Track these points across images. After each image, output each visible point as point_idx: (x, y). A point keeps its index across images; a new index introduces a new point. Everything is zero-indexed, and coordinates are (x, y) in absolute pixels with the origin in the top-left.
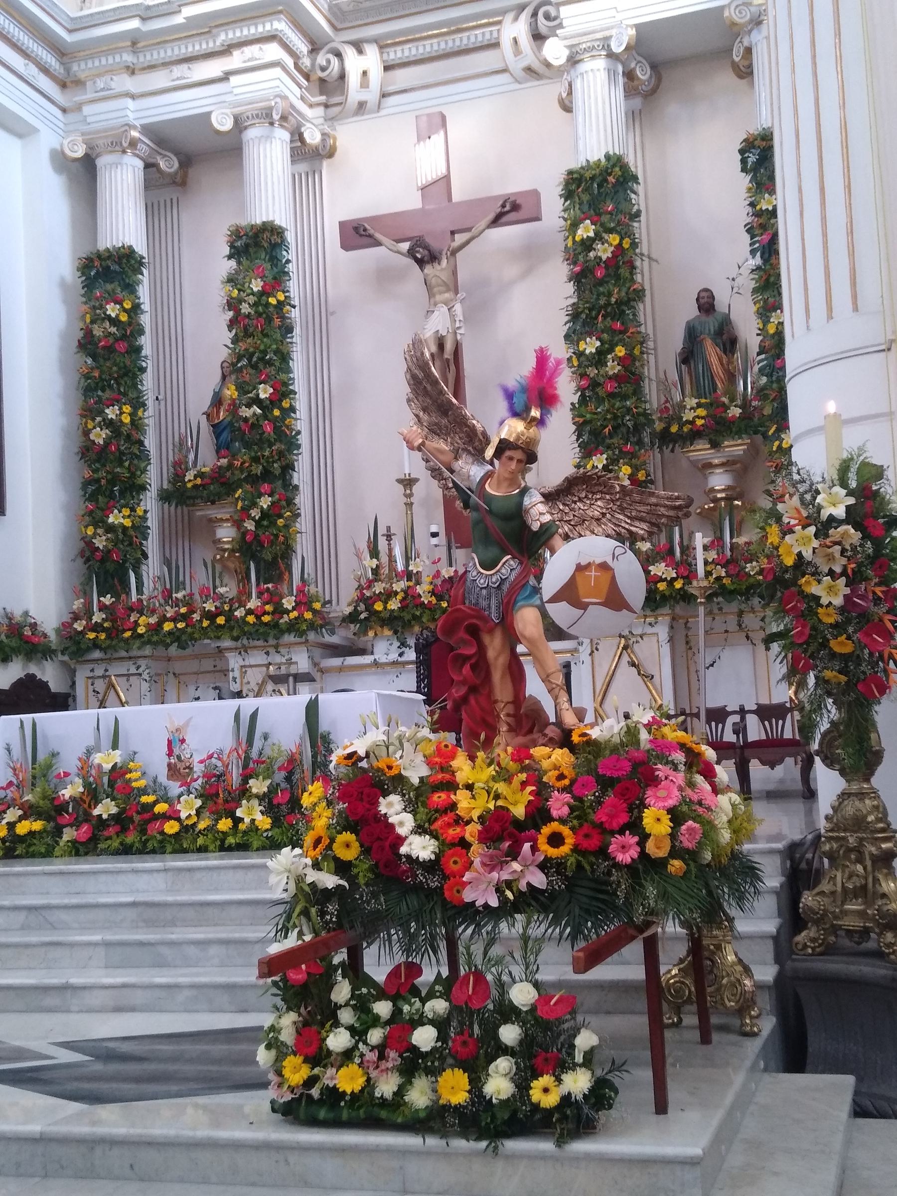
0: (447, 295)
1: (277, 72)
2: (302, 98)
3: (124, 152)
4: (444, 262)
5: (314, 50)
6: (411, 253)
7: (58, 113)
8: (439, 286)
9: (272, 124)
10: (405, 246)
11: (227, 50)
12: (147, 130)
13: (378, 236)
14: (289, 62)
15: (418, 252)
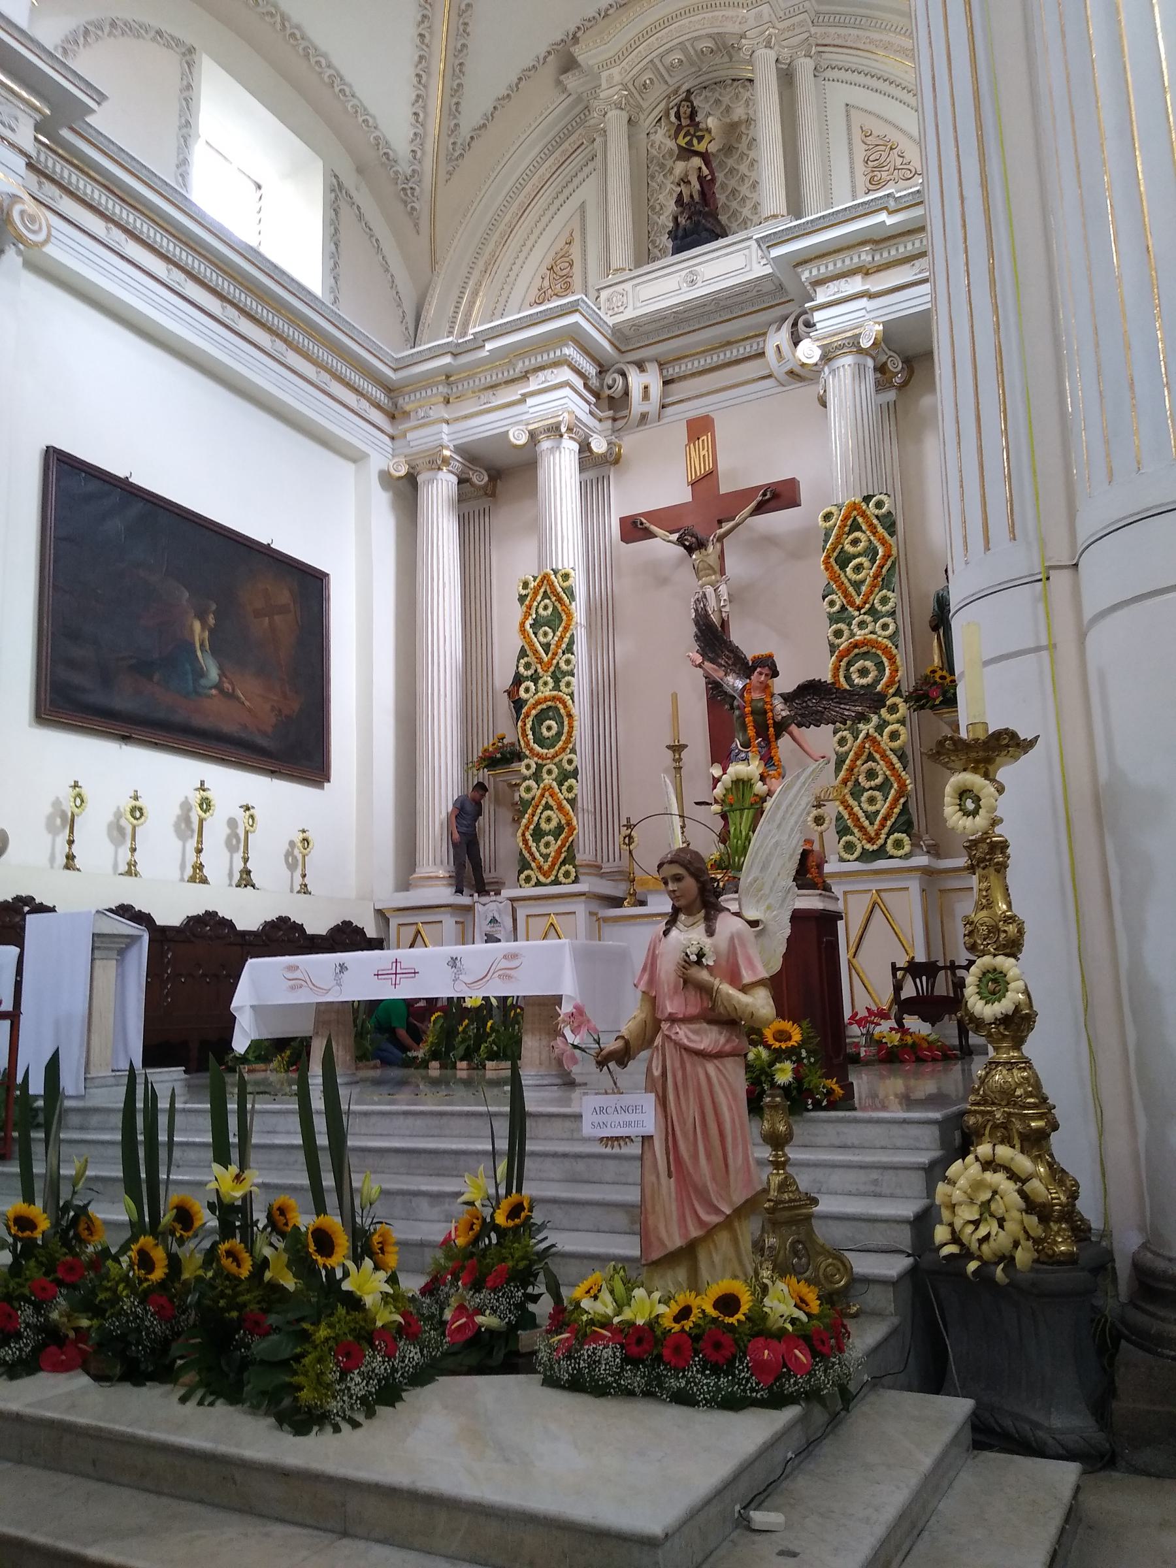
0: (713, 577)
1: (567, 391)
2: (591, 413)
3: (439, 469)
4: (710, 549)
5: (602, 371)
6: (680, 542)
7: (386, 439)
8: (705, 569)
9: (561, 436)
10: (675, 537)
11: (525, 376)
12: (458, 449)
13: (654, 528)
14: (578, 383)
15: (686, 540)
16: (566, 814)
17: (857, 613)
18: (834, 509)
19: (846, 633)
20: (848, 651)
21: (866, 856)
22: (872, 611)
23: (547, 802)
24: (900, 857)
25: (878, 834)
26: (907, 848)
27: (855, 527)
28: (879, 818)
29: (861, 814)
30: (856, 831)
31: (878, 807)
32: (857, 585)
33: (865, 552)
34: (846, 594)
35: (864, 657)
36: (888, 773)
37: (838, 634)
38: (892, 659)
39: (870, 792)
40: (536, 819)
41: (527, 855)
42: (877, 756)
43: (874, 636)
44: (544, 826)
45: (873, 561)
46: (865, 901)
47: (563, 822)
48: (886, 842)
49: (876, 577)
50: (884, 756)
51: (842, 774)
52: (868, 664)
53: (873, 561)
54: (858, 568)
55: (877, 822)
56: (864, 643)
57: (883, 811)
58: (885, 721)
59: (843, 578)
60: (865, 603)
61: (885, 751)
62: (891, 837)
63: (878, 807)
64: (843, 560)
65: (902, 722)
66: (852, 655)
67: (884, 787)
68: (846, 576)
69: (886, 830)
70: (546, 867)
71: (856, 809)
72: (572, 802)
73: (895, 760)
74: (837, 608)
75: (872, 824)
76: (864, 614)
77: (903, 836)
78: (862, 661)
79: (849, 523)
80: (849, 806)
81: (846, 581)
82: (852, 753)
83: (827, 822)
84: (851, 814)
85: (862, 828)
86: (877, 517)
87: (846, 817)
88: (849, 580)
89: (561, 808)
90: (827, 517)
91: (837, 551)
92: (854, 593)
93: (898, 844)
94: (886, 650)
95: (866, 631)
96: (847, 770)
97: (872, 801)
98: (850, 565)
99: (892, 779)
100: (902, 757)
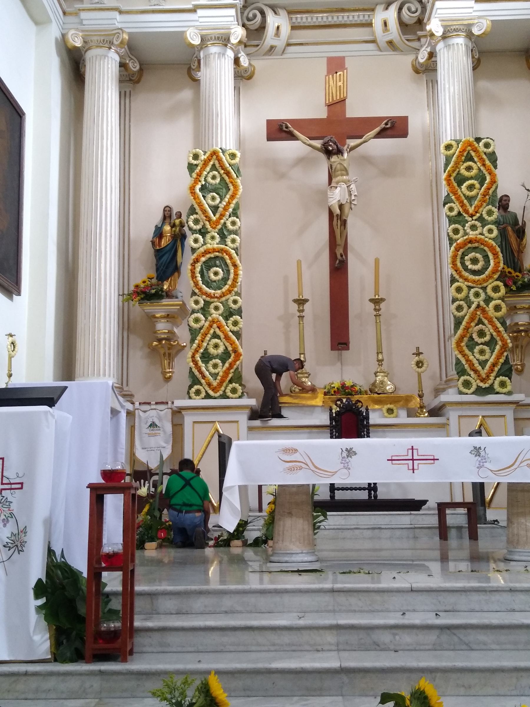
16: (232, 343)
17: (470, 219)
18: (454, 143)
19: (461, 232)
20: (465, 244)
21: (480, 391)
22: (481, 219)
23: (215, 332)
24: (505, 394)
25: (488, 376)
26: (509, 388)
27: (471, 159)
28: (489, 364)
30: (472, 373)
31: (487, 356)
32: (470, 199)
33: (475, 176)
35: (475, 249)
36: (494, 334)
37: (456, 231)
38: (495, 254)
39: (481, 346)
40: (205, 344)
41: (196, 373)
42: (486, 322)
43: (482, 237)
44: (212, 351)
47: (230, 349)
48: (494, 383)
49: (484, 195)
50: (491, 322)
51: (460, 332)
52: (479, 256)
54: (471, 187)
55: (487, 367)
56: (477, 241)
57: (492, 360)
58: (489, 297)
59: (460, 193)
60: (476, 212)
61: (491, 318)
62: (498, 379)
63: (487, 356)
64: (461, 180)
65: (502, 299)
66: (467, 247)
68: (462, 192)
69: (493, 374)
70: (215, 383)
71: (471, 357)
72: (238, 335)
73: (499, 325)
74: (455, 213)
75: (483, 369)
76: (475, 220)
77: (506, 379)
78: (473, 254)
79: (465, 154)
80: (465, 355)
81: (462, 195)
82: (467, 318)
83: (425, 365)
84: (468, 360)
85: (476, 371)
86: (485, 153)
87: (464, 362)
88: (464, 195)
89: (227, 338)
90: (448, 147)
91: (456, 172)
92: (468, 204)
93: (503, 384)
95: (477, 232)
96: (465, 329)
98: (465, 185)
99: (498, 339)
100: (503, 324)
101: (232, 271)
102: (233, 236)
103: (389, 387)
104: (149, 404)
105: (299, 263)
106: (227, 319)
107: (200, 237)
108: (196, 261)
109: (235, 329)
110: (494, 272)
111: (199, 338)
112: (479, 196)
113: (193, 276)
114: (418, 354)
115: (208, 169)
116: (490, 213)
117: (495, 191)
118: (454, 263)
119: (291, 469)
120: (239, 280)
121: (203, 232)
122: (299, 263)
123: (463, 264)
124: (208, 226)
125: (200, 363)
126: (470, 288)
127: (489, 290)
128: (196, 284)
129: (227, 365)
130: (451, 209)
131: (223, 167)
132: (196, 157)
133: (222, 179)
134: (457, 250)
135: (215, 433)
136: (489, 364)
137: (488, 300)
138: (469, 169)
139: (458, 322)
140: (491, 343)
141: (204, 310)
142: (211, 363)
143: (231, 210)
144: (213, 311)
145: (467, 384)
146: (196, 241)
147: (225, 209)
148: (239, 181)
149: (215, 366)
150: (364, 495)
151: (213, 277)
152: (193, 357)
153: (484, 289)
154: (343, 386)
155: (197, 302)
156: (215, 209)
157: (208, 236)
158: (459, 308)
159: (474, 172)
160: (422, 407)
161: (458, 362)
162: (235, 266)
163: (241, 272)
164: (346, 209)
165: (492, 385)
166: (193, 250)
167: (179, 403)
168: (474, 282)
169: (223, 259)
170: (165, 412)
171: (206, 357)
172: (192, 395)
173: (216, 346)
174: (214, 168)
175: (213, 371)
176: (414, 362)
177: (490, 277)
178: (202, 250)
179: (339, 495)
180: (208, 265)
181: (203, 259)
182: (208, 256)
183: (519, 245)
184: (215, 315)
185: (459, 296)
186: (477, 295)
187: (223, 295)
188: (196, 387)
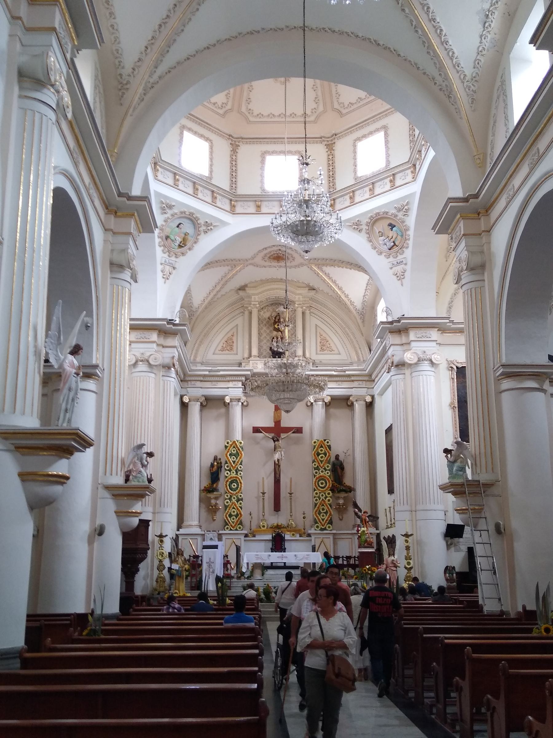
16: (239, 511)
19: (318, 473)
21: (322, 529)
22: (325, 469)
25: (324, 524)
29: (321, 519)
32: (321, 461)
34: (319, 464)
35: (322, 479)
37: (316, 473)
38: (329, 481)
42: (325, 505)
44: (233, 513)
45: (325, 456)
46: (320, 540)
47: (239, 513)
50: (327, 506)
51: (316, 508)
52: (323, 482)
53: (325, 456)
54: (322, 457)
56: (323, 476)
57: (326, 519)
67: (326, 513)
69: (326, 524)
70: (233, 525)
71: (319, 518)
72: (241, 508)
73: (329, 506)
74: (316, 466)
84: (318, 519)
85: (321, 522)
87: (317, 518)
89: (238, 509)
93: (329, 527)
94: (328, 479)
97: (323, 516)
100: (331, 506)
101: (240, 484)
102: (240, 472)
103: (294, 525)
104: (210, 531)
105: (263, 478)
106: (237, 502)
107: (229, 472)
108: (227, 481)
109: (240, 506)
110: (328, 488)
111: (228, 509)
112: (324, 461)
113: (226, 487)
114: (304, 514)
115: (232, 447)
116: (328, 467)
117: (330, 459)
118: (315, 484)
119: (257, 559)
120: (242, 488)
121: (230, 470)
122: (263, 478)
123: (318, 484)
124: (232, 468)
125: (228, 518)
126: (320, 493)
127: (326, 494)
128: (227, 489)
129: (237, 519)
130: (315, 465)
131: (237, 447)
132: (228, 443)
133: (237, 451)
134: (316, 479)
135: (232, 544)
136: (325, 520)
137: (326, 497)
138: (321, 450)
139: (316, 505)
140: (326, 513)
141: (230, 499)
142: (232, 518)
143: (240, 463)
144: (233, 499)
145: (317, 527)
146: (227, 474)
147: (238, 462)
148: (243, 452)
149: (233, 519)
150: (283, 565)
151: (233, 487)
152: (226, 515)
153: (325, 493)
154: (278, 525)
155: (227, 496)
156: (234, 462)
157: (232, 472)
158: (316, 500)
159: (323, 452)
160: (304, 533)
161: (315, 519)
162: (241, 483)
163: (242, 485)
164: (280, 461)
165: (326, 527)
166: (226, 477)
167: (221, 532)
168: (321, 491)
169: (237, 480)
170: (215, 534)
171: (230, 516)
172: (226, 529)
173: (234, 512)
174: (234, 447)
175: (233, 521)
176: (302, 517)
177: (326, 489)
178: (229, 477)
179: (274, 565)
180: (232, 482)
181: (230, 480)
182: (231, 479)
183: (341, 473)
184: (234, 500)
185: (317, 496)
186: (322, 495)
187: (237, 493)
188: (227, 526)
